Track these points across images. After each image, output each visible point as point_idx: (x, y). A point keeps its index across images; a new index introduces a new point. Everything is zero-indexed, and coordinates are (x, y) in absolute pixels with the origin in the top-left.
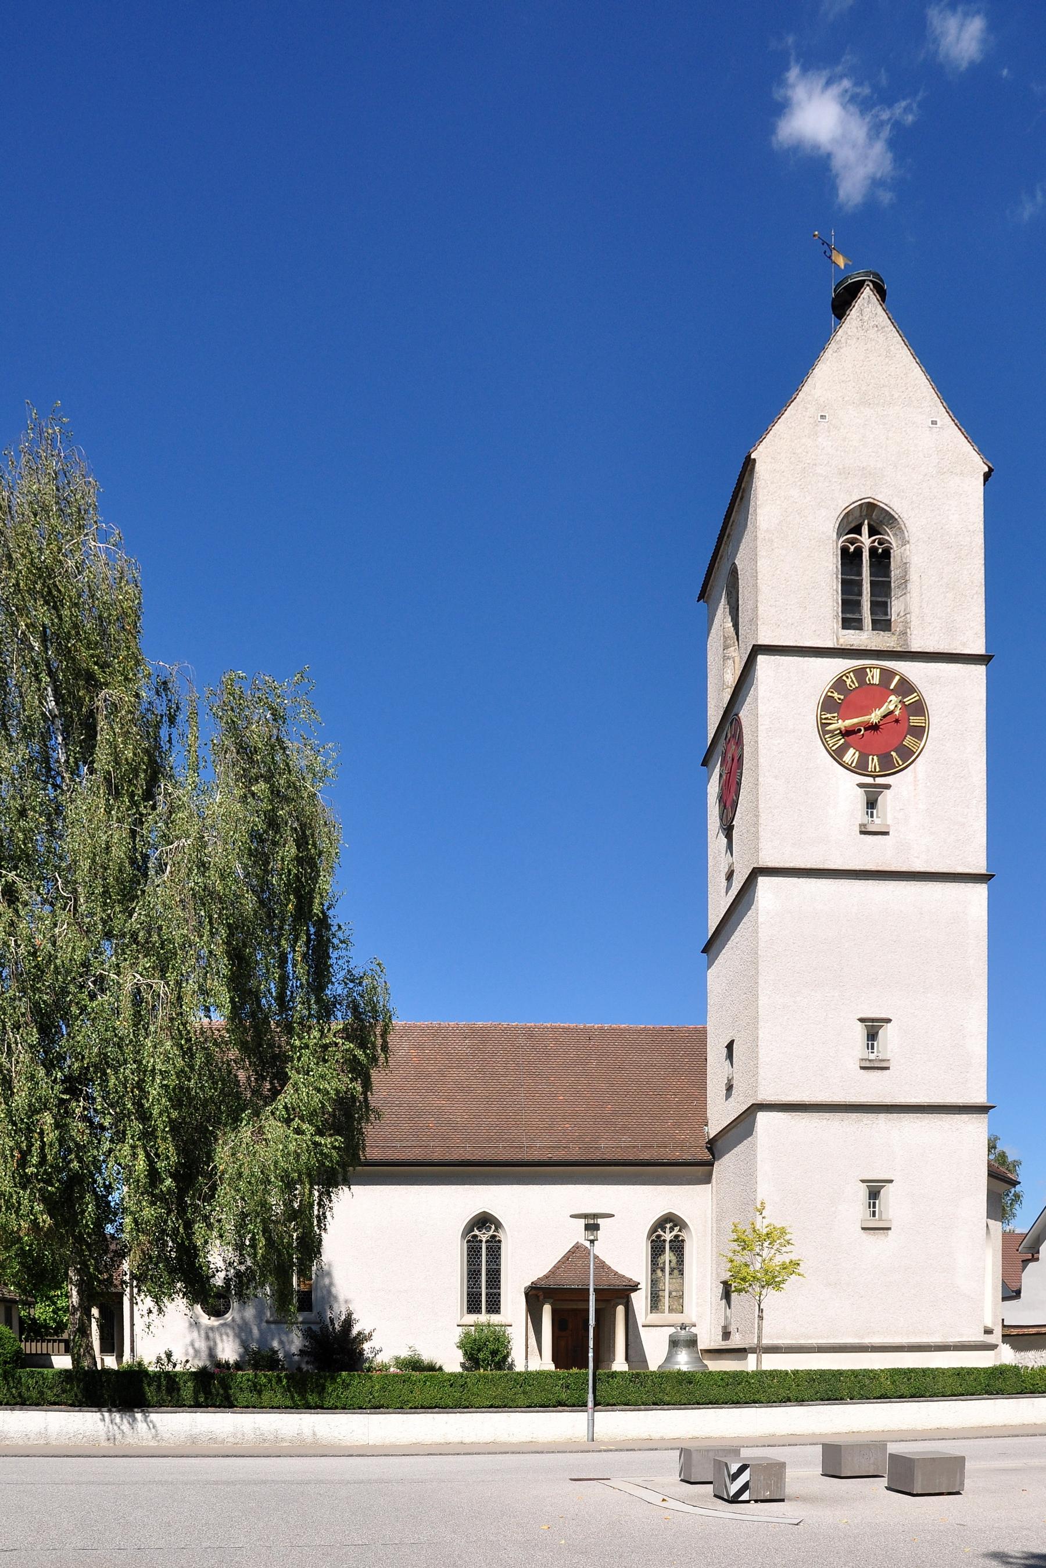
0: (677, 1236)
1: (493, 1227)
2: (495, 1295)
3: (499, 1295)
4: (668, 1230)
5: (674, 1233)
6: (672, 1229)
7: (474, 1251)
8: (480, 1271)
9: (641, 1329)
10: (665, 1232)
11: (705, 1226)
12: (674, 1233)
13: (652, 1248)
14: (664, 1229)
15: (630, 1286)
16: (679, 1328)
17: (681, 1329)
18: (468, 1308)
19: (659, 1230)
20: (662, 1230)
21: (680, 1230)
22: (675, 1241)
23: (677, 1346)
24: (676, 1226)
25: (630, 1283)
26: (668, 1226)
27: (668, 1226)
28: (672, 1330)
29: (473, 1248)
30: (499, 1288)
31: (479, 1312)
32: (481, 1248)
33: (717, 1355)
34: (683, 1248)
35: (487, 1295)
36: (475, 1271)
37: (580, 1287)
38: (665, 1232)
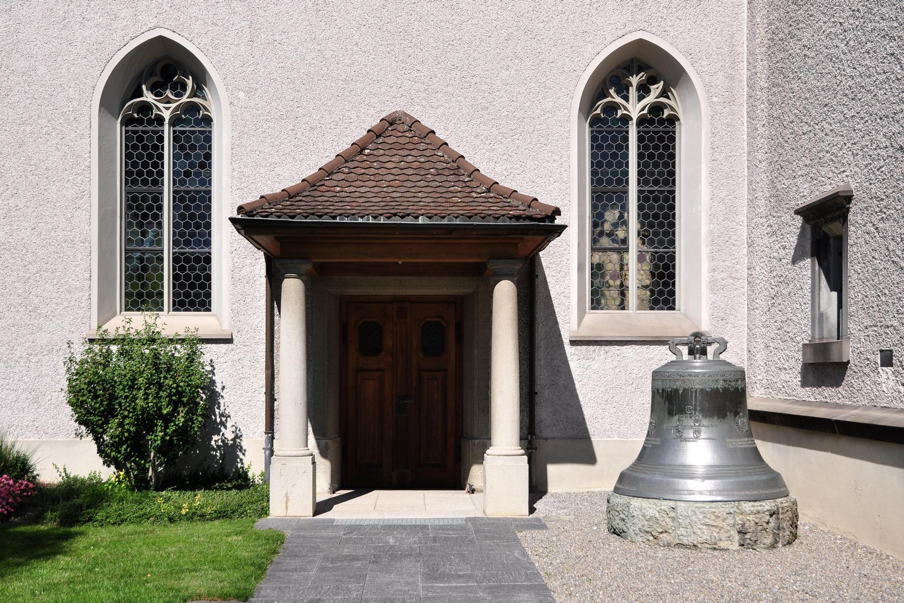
0: (656, 109)
1: (190, 82)
2: (197, 260)
3: (208, 260)
4: (633, 93)
5: (650, 99)
6: (644, 90)
7: (145, 147)
8: (158, 198)
9: (569, 350)
10: (626, 99)
11: (731, 78)
12: (650, 99)
13: (594, 139)
14: (623, 91)
15: (530, 218)
16: (685, 350)
17: (691, 352)
18: (128, 295)
19: (612, 91)
20: (618, 92)
21: (664, 93)
22: (651, 122)
23: (682, 411)
24: (653, 80)
25: (531, 212)
26: (635, 80)
27: (635, 80)
28: (661, 356)
29: (140, 139)
30: (208, 243)
31: (159, 307)
32: (161, 139)
33: (791, 432)
34: (673, 139)
35: (176, 259)
36: (144, 199)
37: (382, 220)
38: (626, 99)
